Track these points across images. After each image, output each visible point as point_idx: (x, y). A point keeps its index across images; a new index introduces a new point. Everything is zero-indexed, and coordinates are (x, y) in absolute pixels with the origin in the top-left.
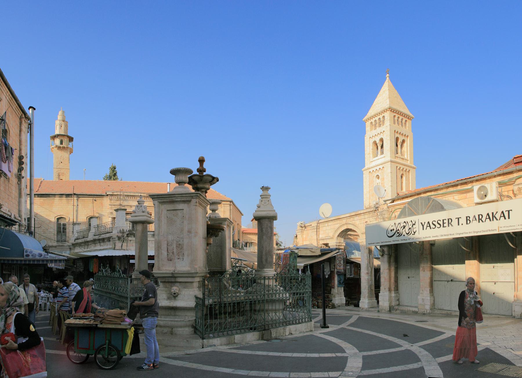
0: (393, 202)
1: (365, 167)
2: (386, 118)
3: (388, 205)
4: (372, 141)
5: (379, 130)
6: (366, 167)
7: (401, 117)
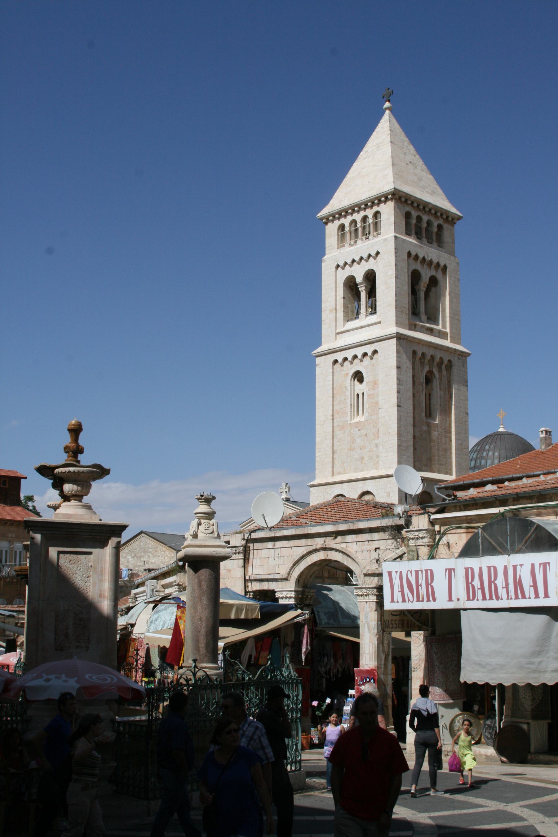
1: (320, 345)
2: (383, 217)
3: (433, 517)
4: (343, 275)
6: (324, 348)
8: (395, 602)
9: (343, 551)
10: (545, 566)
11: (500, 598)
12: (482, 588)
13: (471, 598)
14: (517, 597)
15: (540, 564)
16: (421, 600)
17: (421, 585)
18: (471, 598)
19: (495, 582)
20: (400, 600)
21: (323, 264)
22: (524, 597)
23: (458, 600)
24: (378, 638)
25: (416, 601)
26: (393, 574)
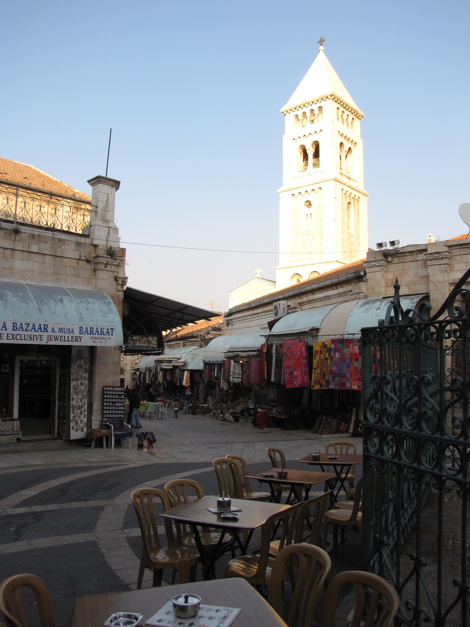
5: (310, 128)
6: (285, 186)
7: (347, 113)
21: (284, 138)
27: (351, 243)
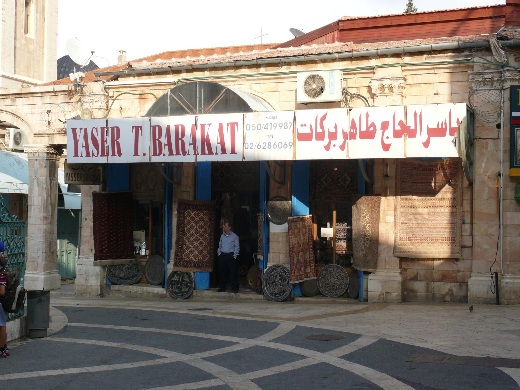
0: (116, 78)
8: (79, 156)
9: (13, 113)
10: (233, 126)
11: (187, 153)
12: (169, 145)
13: (158, 153)
14: (203, 153)
15: (228, 124)
16: (105, 155)
17: (106, 141)
18: (158, 153)
19: (182, 139)
20: (84, 154)
22: (211, 152)
23: (144, 154)
24: (46, 192)
25: (101, 156)
26: (78, 131)
27: (29, 52)
